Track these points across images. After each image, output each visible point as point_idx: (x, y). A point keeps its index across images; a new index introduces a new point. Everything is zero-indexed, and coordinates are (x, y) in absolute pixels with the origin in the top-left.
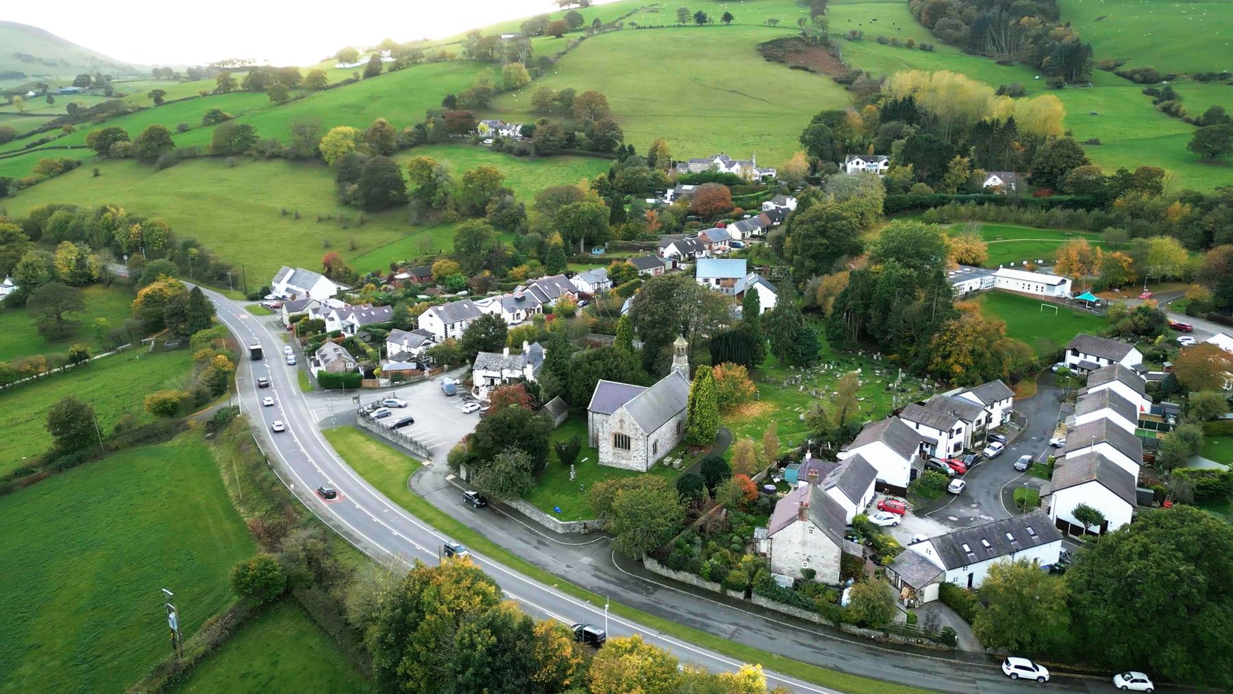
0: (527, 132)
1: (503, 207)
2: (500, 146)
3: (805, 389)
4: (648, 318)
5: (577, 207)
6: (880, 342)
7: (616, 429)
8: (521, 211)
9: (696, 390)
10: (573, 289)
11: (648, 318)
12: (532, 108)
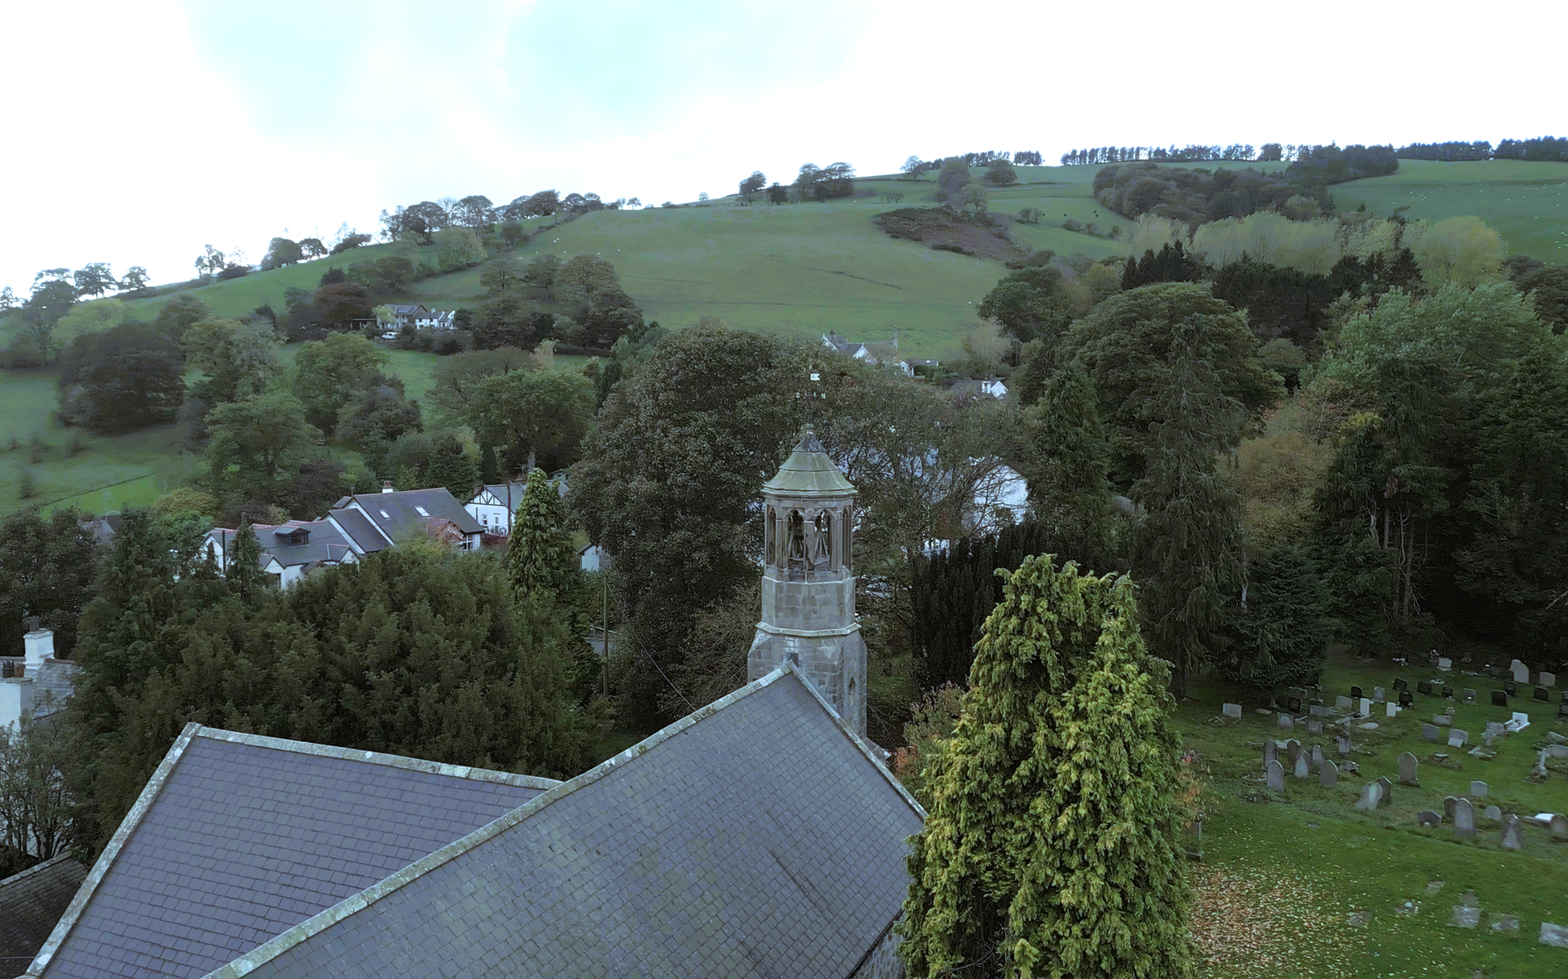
0: (462, 318)
1: (372, 408)
2: (410, 341)
3: (1385, 801)
4: (640, 485)
5: (520, 378)
8: (411, 418)
9: (1006, 790)
10: (471, 529)
11: (640, 485)
12: (485, 290)
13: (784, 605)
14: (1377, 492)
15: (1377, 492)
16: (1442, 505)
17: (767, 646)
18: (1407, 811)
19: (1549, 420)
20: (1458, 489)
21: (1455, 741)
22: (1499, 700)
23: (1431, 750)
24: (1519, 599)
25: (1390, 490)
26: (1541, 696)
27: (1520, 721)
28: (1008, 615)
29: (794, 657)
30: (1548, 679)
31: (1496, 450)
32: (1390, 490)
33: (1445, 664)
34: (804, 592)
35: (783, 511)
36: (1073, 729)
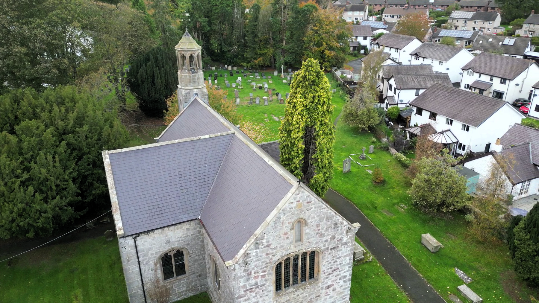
6: (229, 55)
7: (285, 247)
13: (192, 81)
14: (195, 27)
15: (195, 27)
16: (209, 28)
17: (189, 93)
18: (246, 103)
19: (227, 5)
20: (210, 23)
21: (234, 86)
22: (232, 75)
23: (230, 89)
24: (226, 50)
25: (198, 25)
26: (237, 72)
27: (239, 79)
28: (305, 72)
29: (197, 94)
30: (235, 68)
31: (217, 13)
32: (198, 25)
33: (214, 69)
34: (197, 76)
35: (188, 55)
36: (322, 91)
